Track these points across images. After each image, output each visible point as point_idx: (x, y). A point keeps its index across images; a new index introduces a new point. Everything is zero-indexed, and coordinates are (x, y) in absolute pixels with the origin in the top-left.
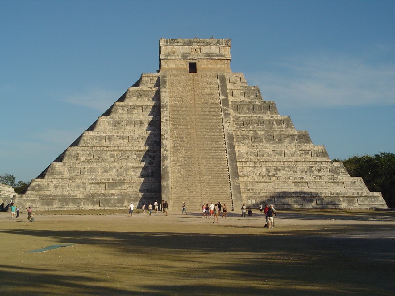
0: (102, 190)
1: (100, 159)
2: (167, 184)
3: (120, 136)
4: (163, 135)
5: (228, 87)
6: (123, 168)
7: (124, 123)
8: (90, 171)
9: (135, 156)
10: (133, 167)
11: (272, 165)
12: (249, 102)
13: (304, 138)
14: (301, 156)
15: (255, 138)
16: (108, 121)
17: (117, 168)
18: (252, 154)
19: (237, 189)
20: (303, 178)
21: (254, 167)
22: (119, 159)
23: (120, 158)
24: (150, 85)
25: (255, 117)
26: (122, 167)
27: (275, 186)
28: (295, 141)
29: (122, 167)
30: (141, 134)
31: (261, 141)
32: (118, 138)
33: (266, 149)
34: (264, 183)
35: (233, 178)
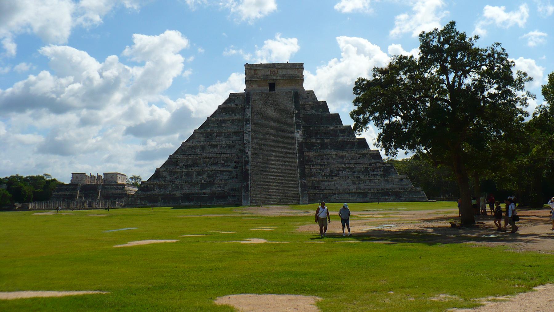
0: (197, 190)
1: (195, 164)
2: (248, 185)
4: (245, 144)
5: (300, 103)
7: (214, 135)
9: (223, 162)
12: (318, 115)
20: (359, 177)
21: (320, 169)
24: (236, 102)
35: (300, 179)
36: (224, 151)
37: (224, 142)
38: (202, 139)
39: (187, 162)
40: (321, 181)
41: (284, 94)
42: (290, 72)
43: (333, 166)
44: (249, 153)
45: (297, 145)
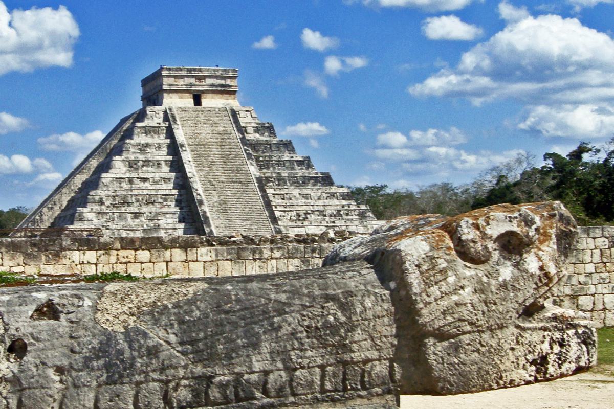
1: (125, 203)
2: (211, 231)
3: (141, 178)
7: (140, 163)
8: (120, 216)
9: (161, 201)
12: (266, 141)
13: (327, 180)
14: (327, 199)
15: (279, 180)
16: (123, 161)
17: (147, 213)
21: (284, 211)
25: (275, 156)
28: (319, 184)
36: (158, 187)
37: (157, 175)
38: (124, 169)
39: (114, 200)
40: (290, 226)
41: (217, 110)
43: (299, 208)
44: (200, 191)
45: (255, 180)
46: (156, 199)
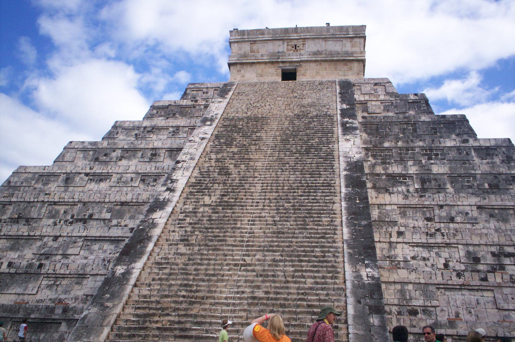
2: (127, 273)
3: (94, 174)
6: (60, 239)
9: (108, 216)
10: (86, 236)
11: (483, 242)
15: (423, 182)
17: (45, 239)
18: (418, 214)
19: (372, 298)
22: (66, 221)
23: (71, 220)
26: (60, 236)
27: (506, 300)
29: (60, 236)
30: (142, 171)
31: (440, 189)
32: (87, 178)
33: (459, 203)
34: (464, 292)
40: (438, 286)
42: (334, 46)
45: (343, 165)
46: (95, 211)
